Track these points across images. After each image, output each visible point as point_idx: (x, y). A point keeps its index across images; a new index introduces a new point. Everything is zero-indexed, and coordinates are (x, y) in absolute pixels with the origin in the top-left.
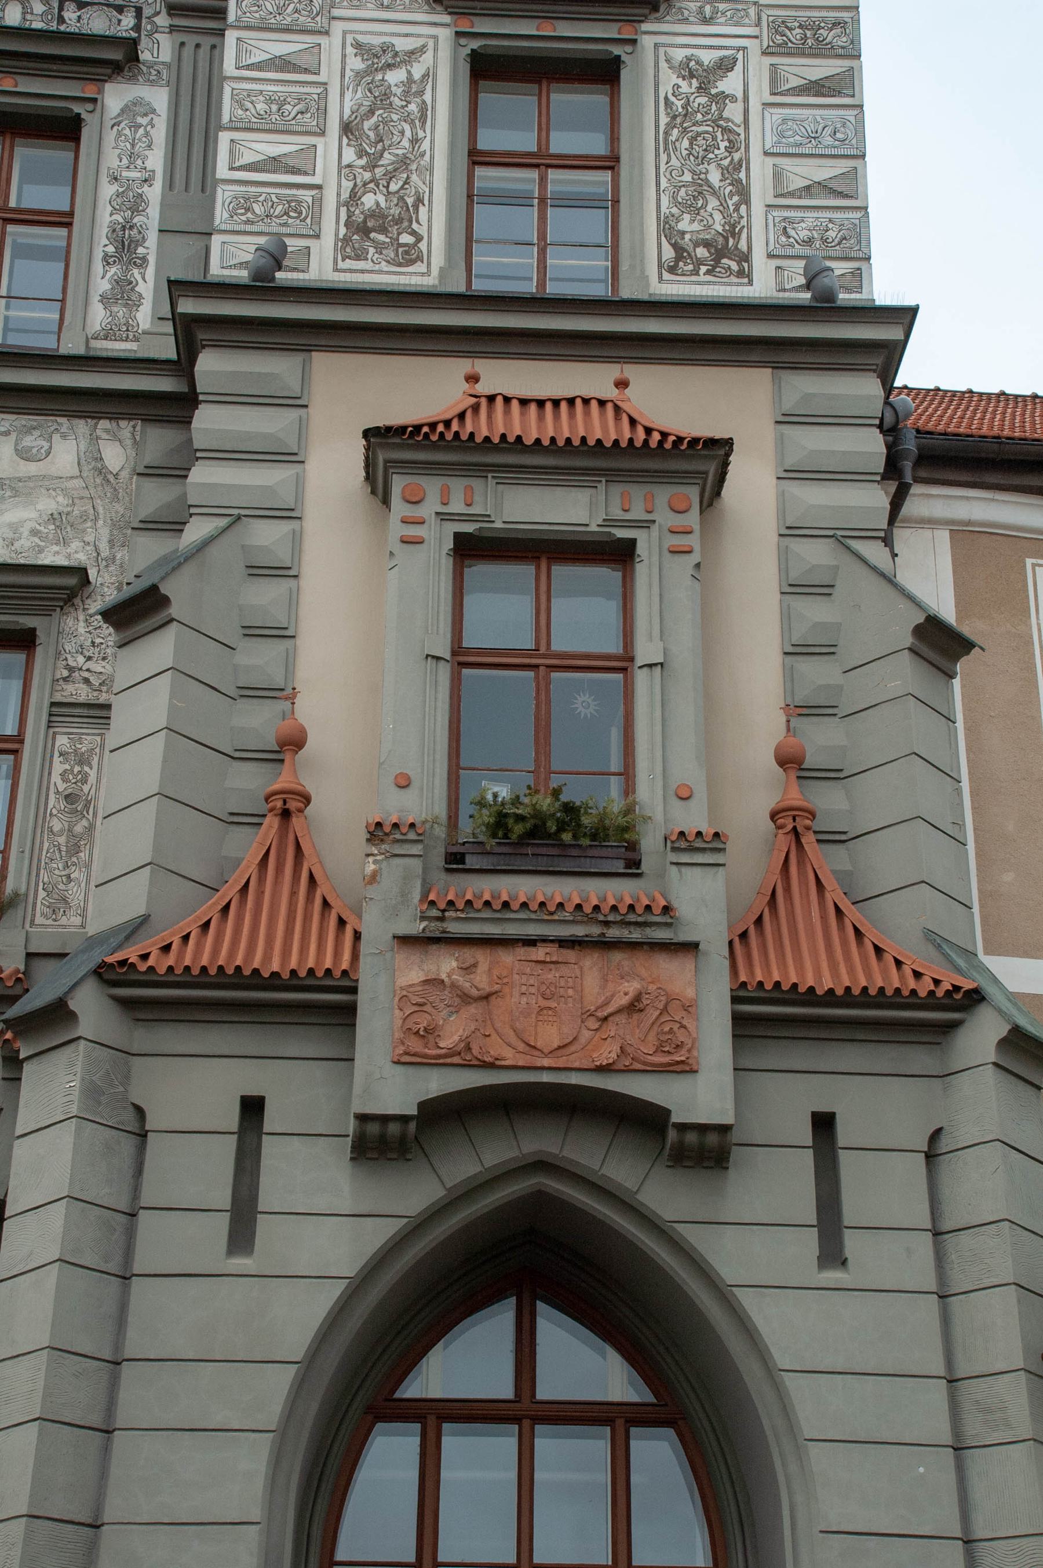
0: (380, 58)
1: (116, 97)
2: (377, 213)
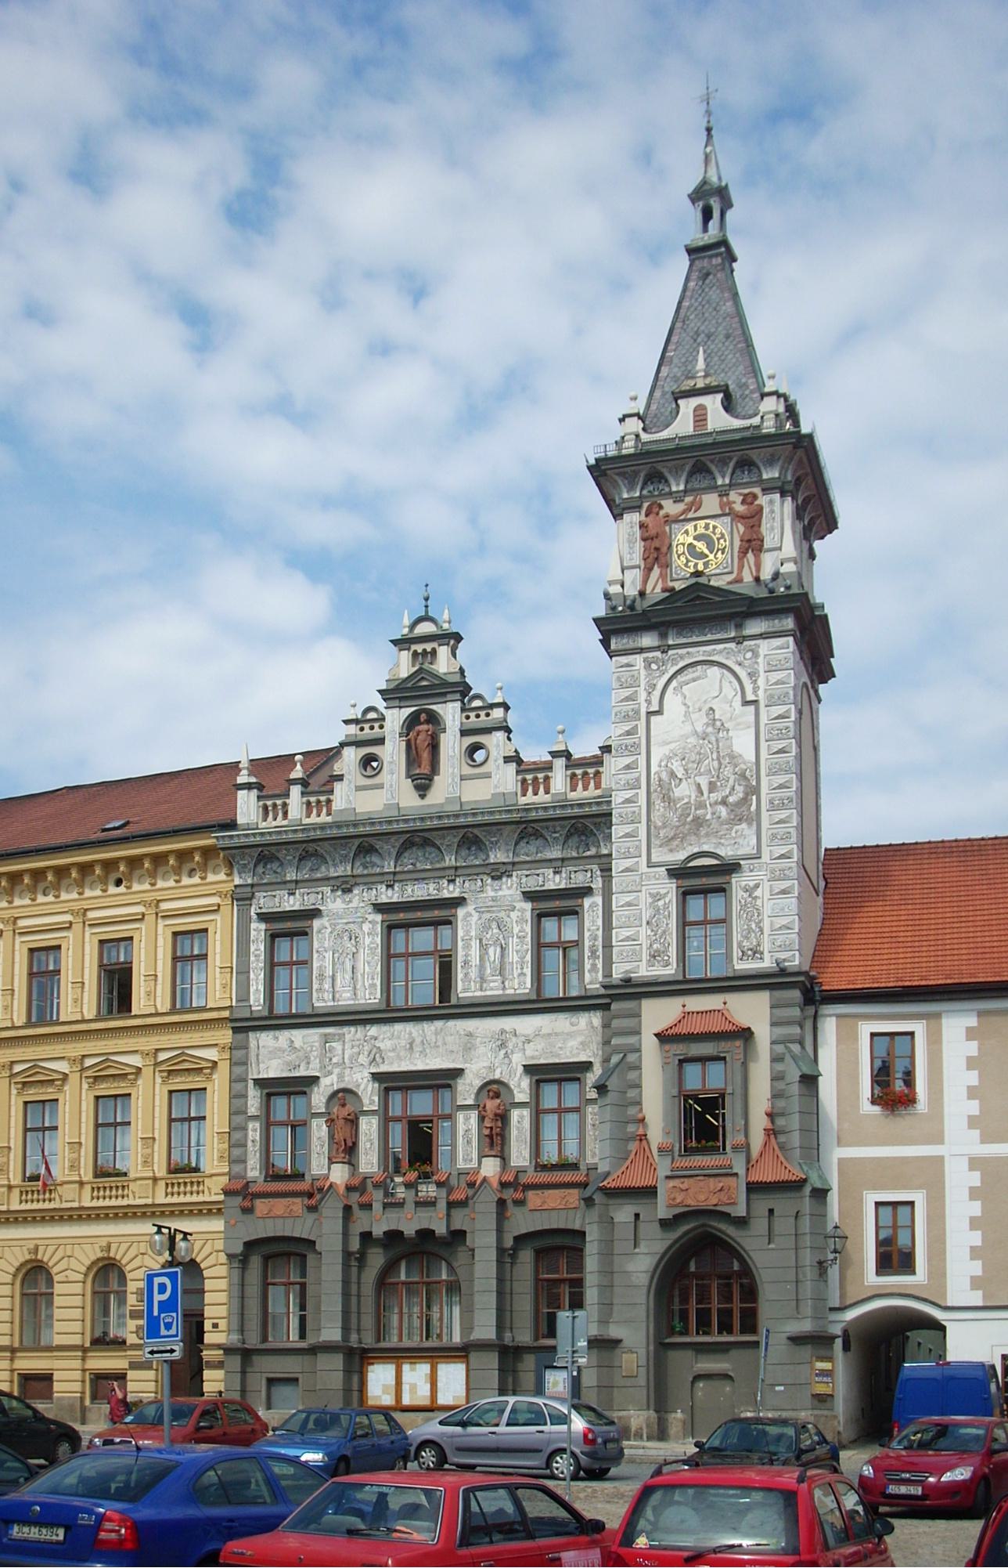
0: (657, 897)
1: (587, 902)
2: (657, 951)
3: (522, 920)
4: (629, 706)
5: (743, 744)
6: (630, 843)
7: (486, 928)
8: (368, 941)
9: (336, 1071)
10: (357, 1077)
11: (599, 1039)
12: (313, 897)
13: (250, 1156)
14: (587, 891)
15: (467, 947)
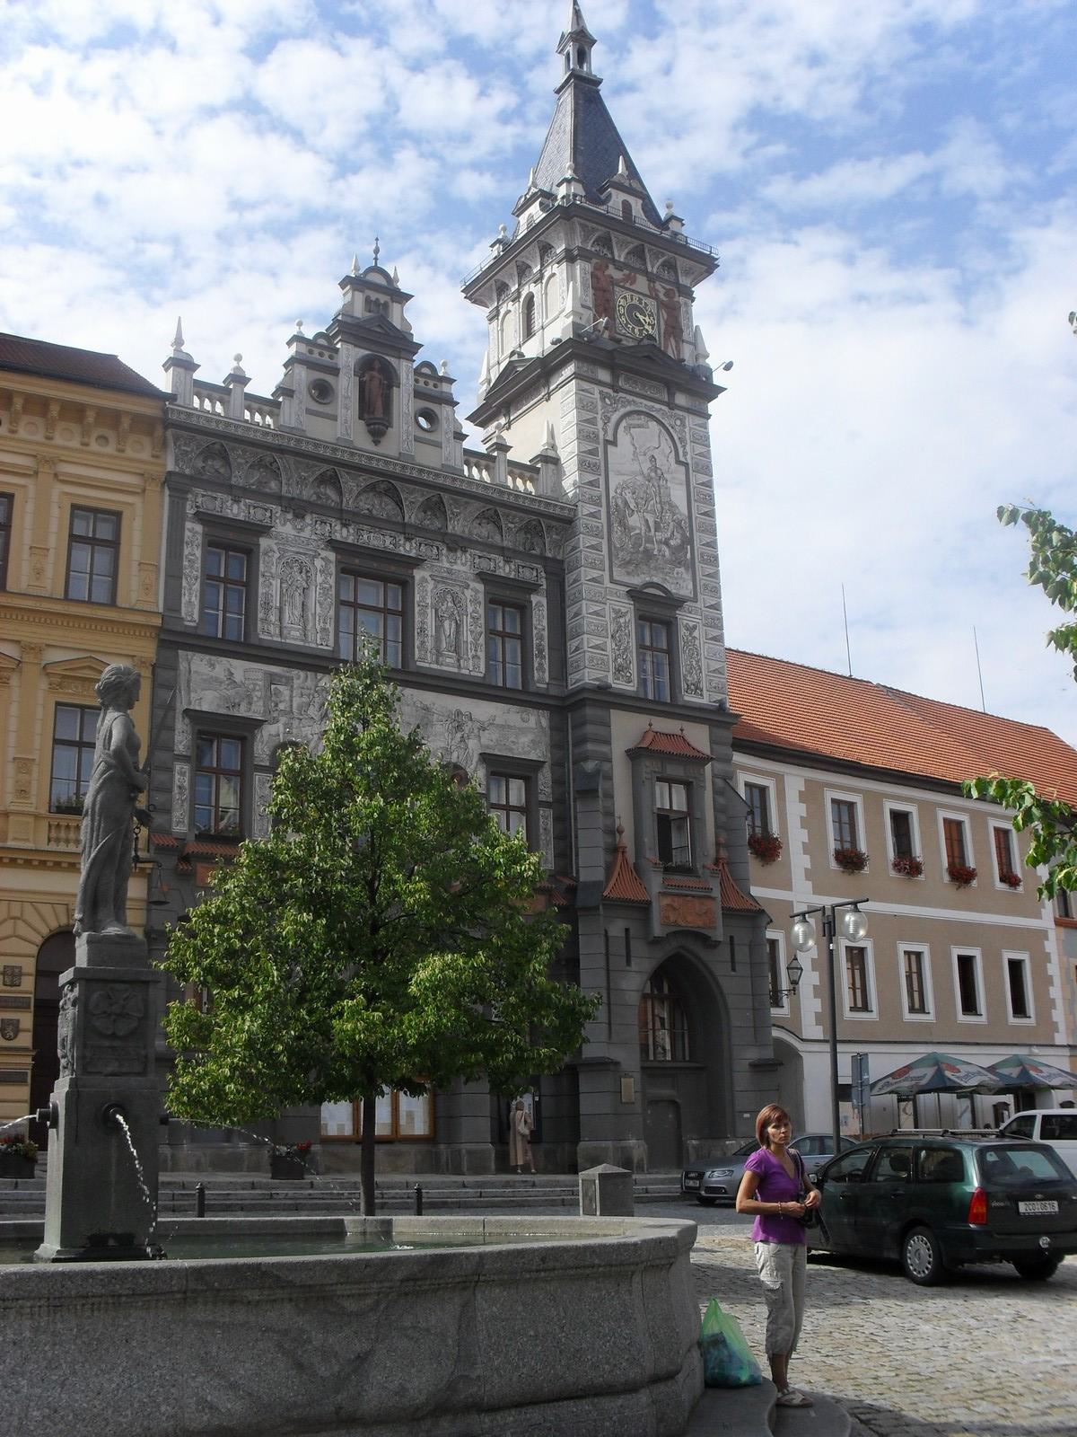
0: (619, 615)
1: (535, 599)
3: (474, 601)
4: (590, 428)
5: (678, 496)
6: (593, 554)
7: (441, 598)
8: (320, 579)
9: (283, 719)
10: (307, 731)
11: (547, 740)
12: (260, 512)
13: (176, 806)
14: (533, 588)
15: (423, 614)
